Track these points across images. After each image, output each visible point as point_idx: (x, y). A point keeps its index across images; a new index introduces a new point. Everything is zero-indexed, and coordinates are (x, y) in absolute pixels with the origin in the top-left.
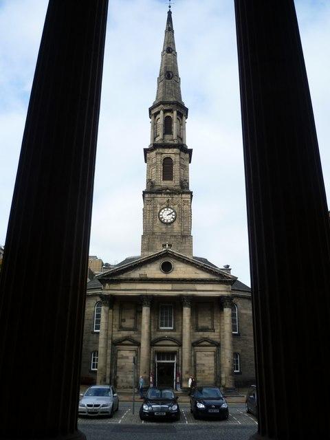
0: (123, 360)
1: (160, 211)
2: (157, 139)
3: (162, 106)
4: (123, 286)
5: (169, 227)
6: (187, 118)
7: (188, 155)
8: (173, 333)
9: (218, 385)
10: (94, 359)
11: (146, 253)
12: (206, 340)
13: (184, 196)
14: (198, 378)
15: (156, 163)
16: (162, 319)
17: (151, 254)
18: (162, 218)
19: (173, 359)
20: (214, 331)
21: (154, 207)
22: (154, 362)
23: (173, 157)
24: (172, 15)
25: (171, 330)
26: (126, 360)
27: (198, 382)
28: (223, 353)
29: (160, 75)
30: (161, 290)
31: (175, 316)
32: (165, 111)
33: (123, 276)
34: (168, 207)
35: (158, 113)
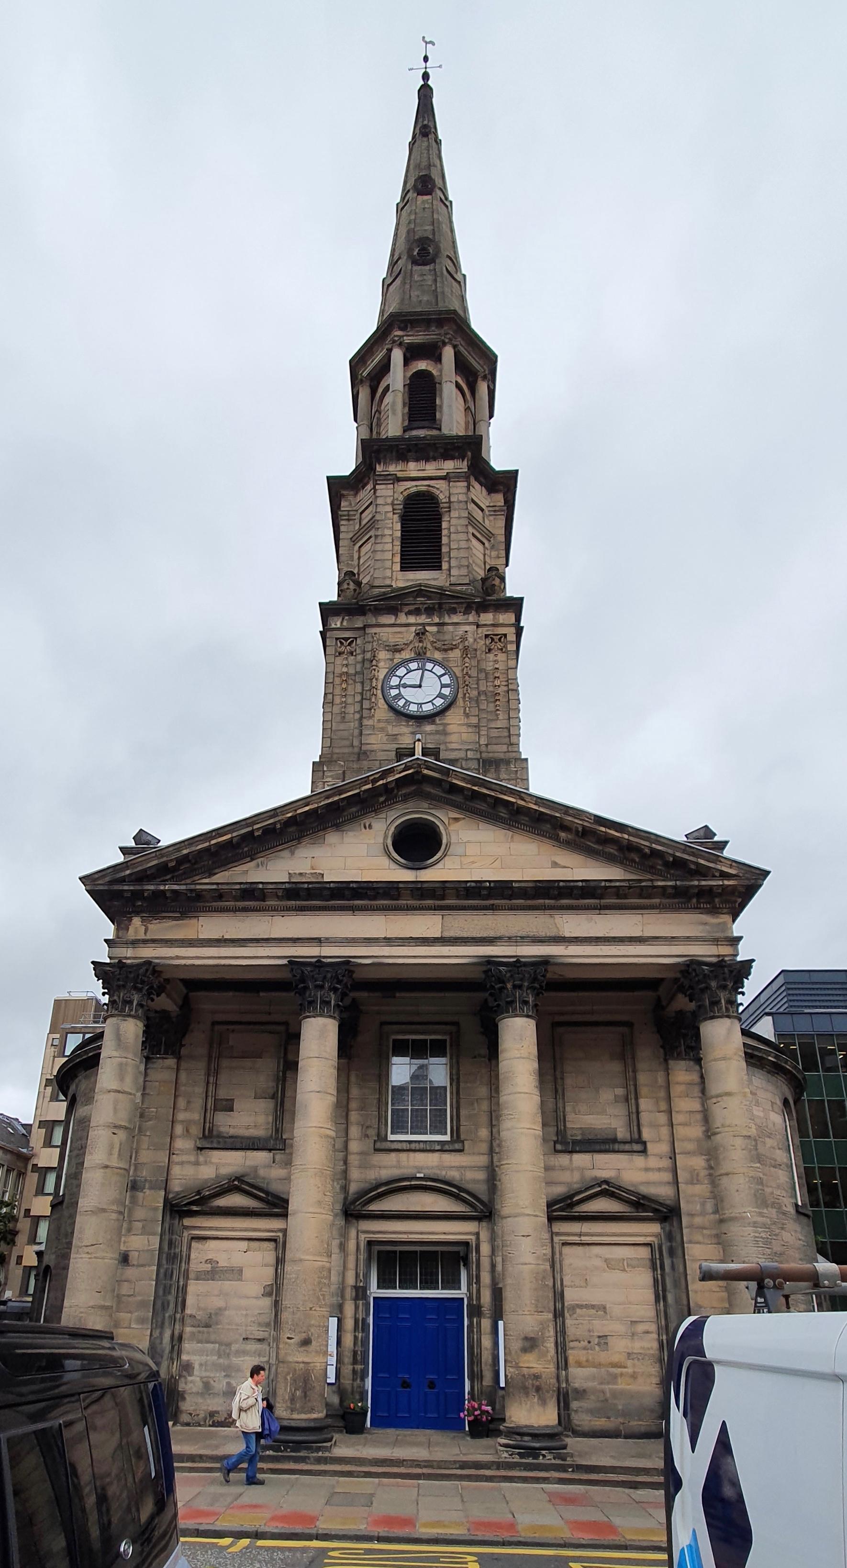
13: (487, 618)
22: (360, 1292)
26: (228, 1285)
27: (581, 1394)
30: (388, 941)
34: (420, 656)
35: (384, 368)
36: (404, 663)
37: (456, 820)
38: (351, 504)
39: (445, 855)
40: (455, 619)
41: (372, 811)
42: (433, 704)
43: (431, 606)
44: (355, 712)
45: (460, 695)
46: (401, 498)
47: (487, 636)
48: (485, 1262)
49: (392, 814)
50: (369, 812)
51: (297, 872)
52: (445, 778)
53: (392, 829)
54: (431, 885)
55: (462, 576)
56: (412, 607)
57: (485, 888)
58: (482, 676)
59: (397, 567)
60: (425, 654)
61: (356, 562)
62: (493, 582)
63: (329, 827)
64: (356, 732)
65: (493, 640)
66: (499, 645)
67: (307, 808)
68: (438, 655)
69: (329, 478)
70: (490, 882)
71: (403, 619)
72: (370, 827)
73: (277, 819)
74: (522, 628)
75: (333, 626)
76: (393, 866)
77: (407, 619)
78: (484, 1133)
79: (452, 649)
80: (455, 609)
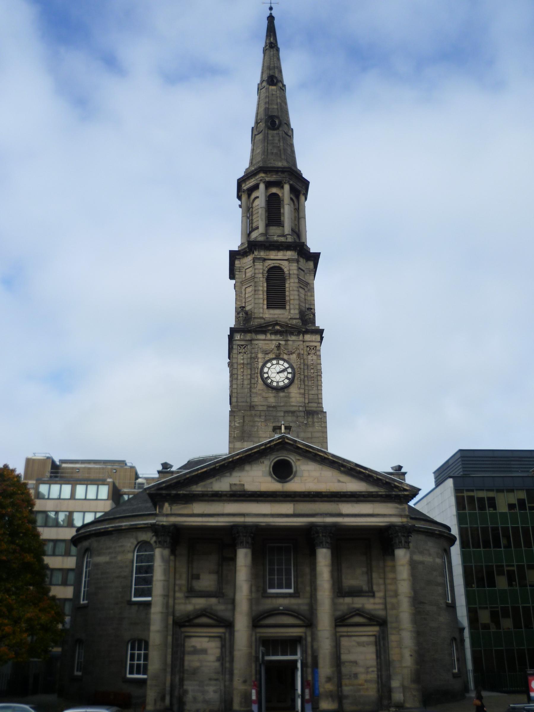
0: (195, 657)
1: (264, 365)
2: (254, 235)
3: (262, 175)
4: (198, 508)
5: (282, 394)
6: (306, 199)
7: (311, 264)
8: (294, 601)
9: (385, 702)
10: (132, 656)
11: (238, 445)
12: (359, 612)
13: (308, 337)
14: (347, 690)
15: (253, 277)
16: (271, 572)
17: (248, 446)
18: (268, 377)
19: (295, 653)
20: (373, 596)
21: (251, 358)
23: (285, 265)
24: (276, 22)
25: (290, 596)
27: (347, 697)
28: (393, 638)
29: (257, 123)
31: (296, 565)
32: (269, 185)
33: (198, 488)
34: (278, 358)
35: (256, 187)
36: (270, 360)
37: (299, 460)
38: (240, 263)
39: (295, 476)
42: (284, 382)
43: (282, 331)
44: (247, 385)
45: (296, 378)
46: (266, 269)
47: (307, 346)
48: (309, 645)
49: (272, 457)
51: (233, 483)
52: (295, 444)
53: (272, 464)
55: (296, 314)
58: (306, 367)
59: (265, 307)
60: (280, 356)
61: (243, 295)
62: (310, 317)
64: (249, 395)
65: (310, 348)
66: (313, 351)
67: (238, 457)
68: (285, 357)
69: (230, 251)
70: (313, 492)
71: (269, 336)
72: (263, 462)
73: (225, 462)
74: (323, 337)
75: (236, 338)
76: (273, 481)
78: (308, 589)
79: (292, 354)
80: (293, 332)
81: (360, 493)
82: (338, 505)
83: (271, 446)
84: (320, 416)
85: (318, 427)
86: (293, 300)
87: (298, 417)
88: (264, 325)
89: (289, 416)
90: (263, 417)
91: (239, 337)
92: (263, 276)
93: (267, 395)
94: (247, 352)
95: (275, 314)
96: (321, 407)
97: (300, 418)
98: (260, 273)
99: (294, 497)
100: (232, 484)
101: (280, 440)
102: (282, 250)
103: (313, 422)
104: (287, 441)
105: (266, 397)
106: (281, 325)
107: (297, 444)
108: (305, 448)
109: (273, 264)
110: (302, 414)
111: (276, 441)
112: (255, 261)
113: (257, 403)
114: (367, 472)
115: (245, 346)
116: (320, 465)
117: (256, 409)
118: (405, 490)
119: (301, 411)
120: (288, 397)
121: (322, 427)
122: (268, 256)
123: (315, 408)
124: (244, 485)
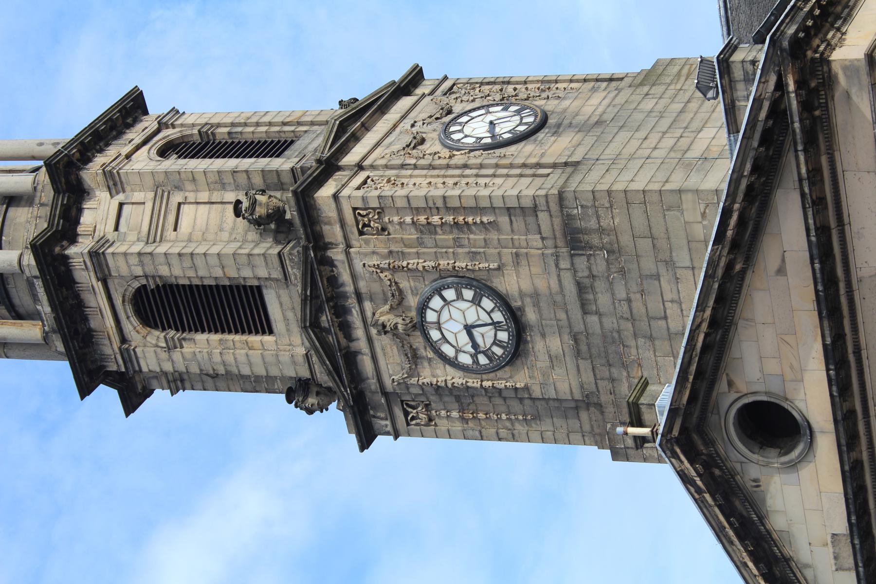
1: (453, 363)
5: (531, 316)
34: (420, 326)
37: (730, 384)
40: (345, 277)
41: (735, 480)
47: (361, 233)
49: (733, 455)
50: (737, 483)
51: (833, 561)
53: (755, 457)
54: (842, 435)
56: (341, 335)
57: (837, 374)
63: (765, 528)
67: (751, 565)
68: (413, 301)
70: (828, 370)
71: (362, 344)
72: (755, 481)
77: (358, 339)
80: (328, 279)
81: (813, 233)
82: (860, 281)
83: (699, 475)
84: (575, 211)
85: (612, 218)
86: (226, 270)
87: (595, 273)
88: (328, 362)
89: (595, 300)
90: (613, 370)
91: (383, 423)
92: (175, 347)
93: (543, 362)
94: (423, 402)
95: (286, 319)
96: (547, 202)
97: (594, 267)
98: (170, 356)
99: (852, 412)
100: (836, 564)
101: (678, 451)
102: (77, 296)
103: (601, 231)
104: (676, 432)
105: (550, 357)
106: (313, 312)
107: (682, 406)
108: (689, 386)
109: (128, 318)
110: (581, 263)
111: (682, 462)
112: (137, 368)
113: (575, 384)
114: (737, 206)
115: (405, 406)
116: (737, 325)
117: (594, 389)
118: (780, 85)
119: (572, 264)
120: (536, 296)
121: (611, 207)
122: (111, 333)
123: (554, 219)
124: (834, 535)
